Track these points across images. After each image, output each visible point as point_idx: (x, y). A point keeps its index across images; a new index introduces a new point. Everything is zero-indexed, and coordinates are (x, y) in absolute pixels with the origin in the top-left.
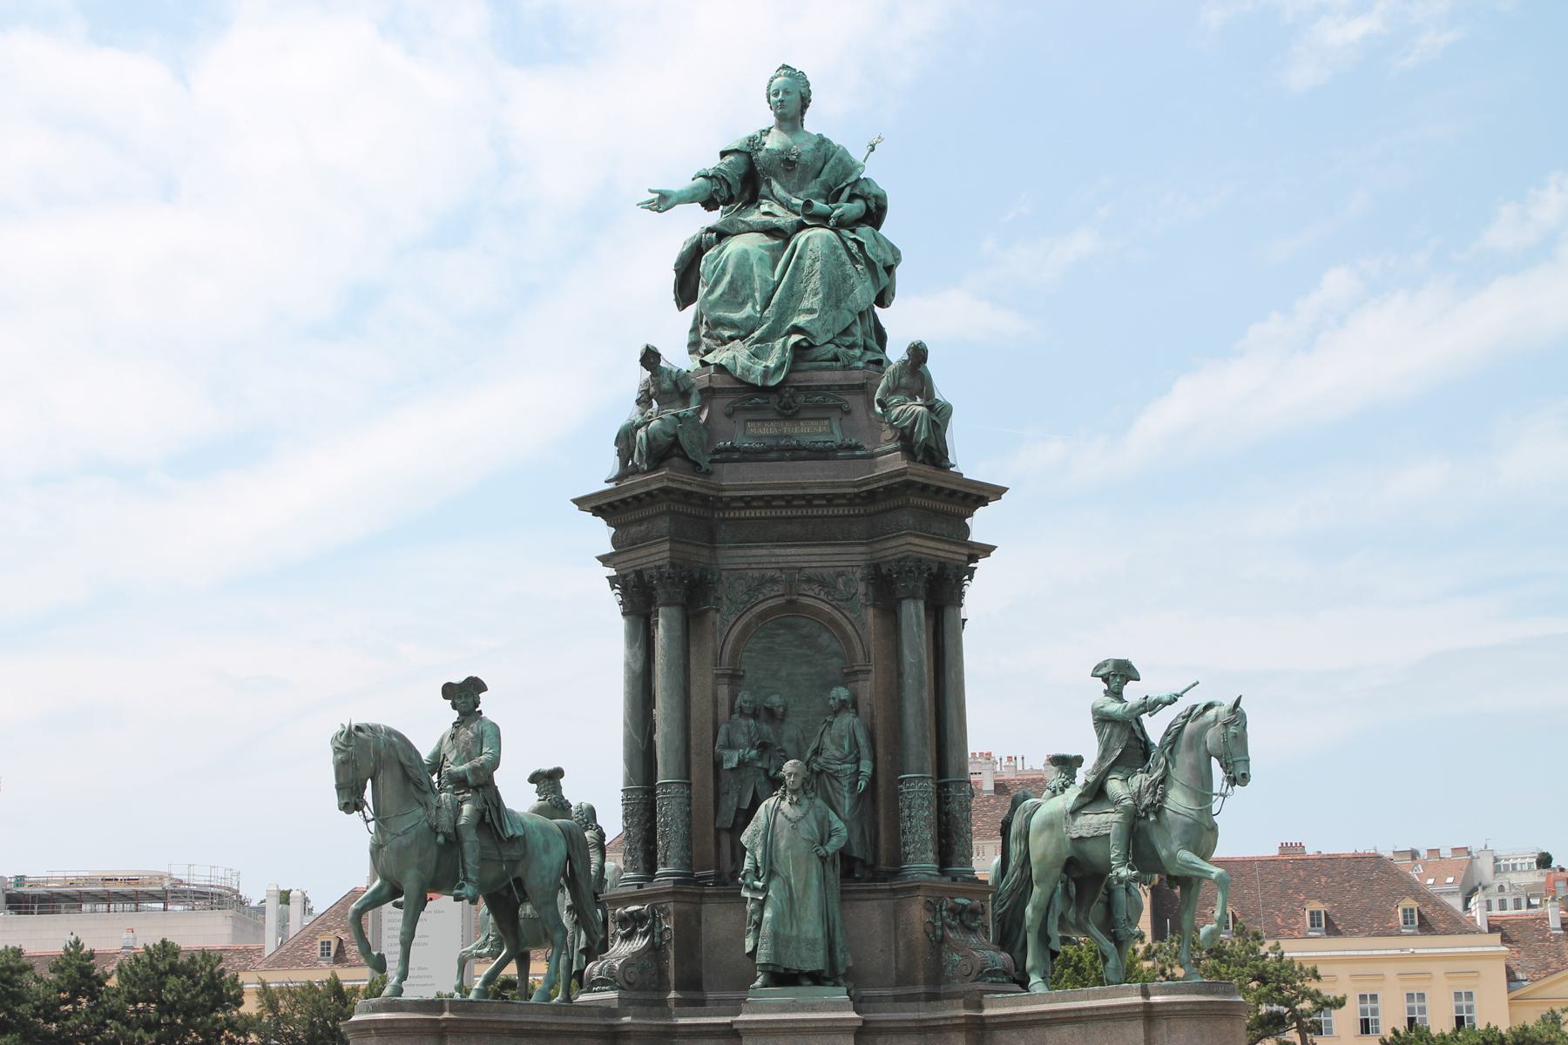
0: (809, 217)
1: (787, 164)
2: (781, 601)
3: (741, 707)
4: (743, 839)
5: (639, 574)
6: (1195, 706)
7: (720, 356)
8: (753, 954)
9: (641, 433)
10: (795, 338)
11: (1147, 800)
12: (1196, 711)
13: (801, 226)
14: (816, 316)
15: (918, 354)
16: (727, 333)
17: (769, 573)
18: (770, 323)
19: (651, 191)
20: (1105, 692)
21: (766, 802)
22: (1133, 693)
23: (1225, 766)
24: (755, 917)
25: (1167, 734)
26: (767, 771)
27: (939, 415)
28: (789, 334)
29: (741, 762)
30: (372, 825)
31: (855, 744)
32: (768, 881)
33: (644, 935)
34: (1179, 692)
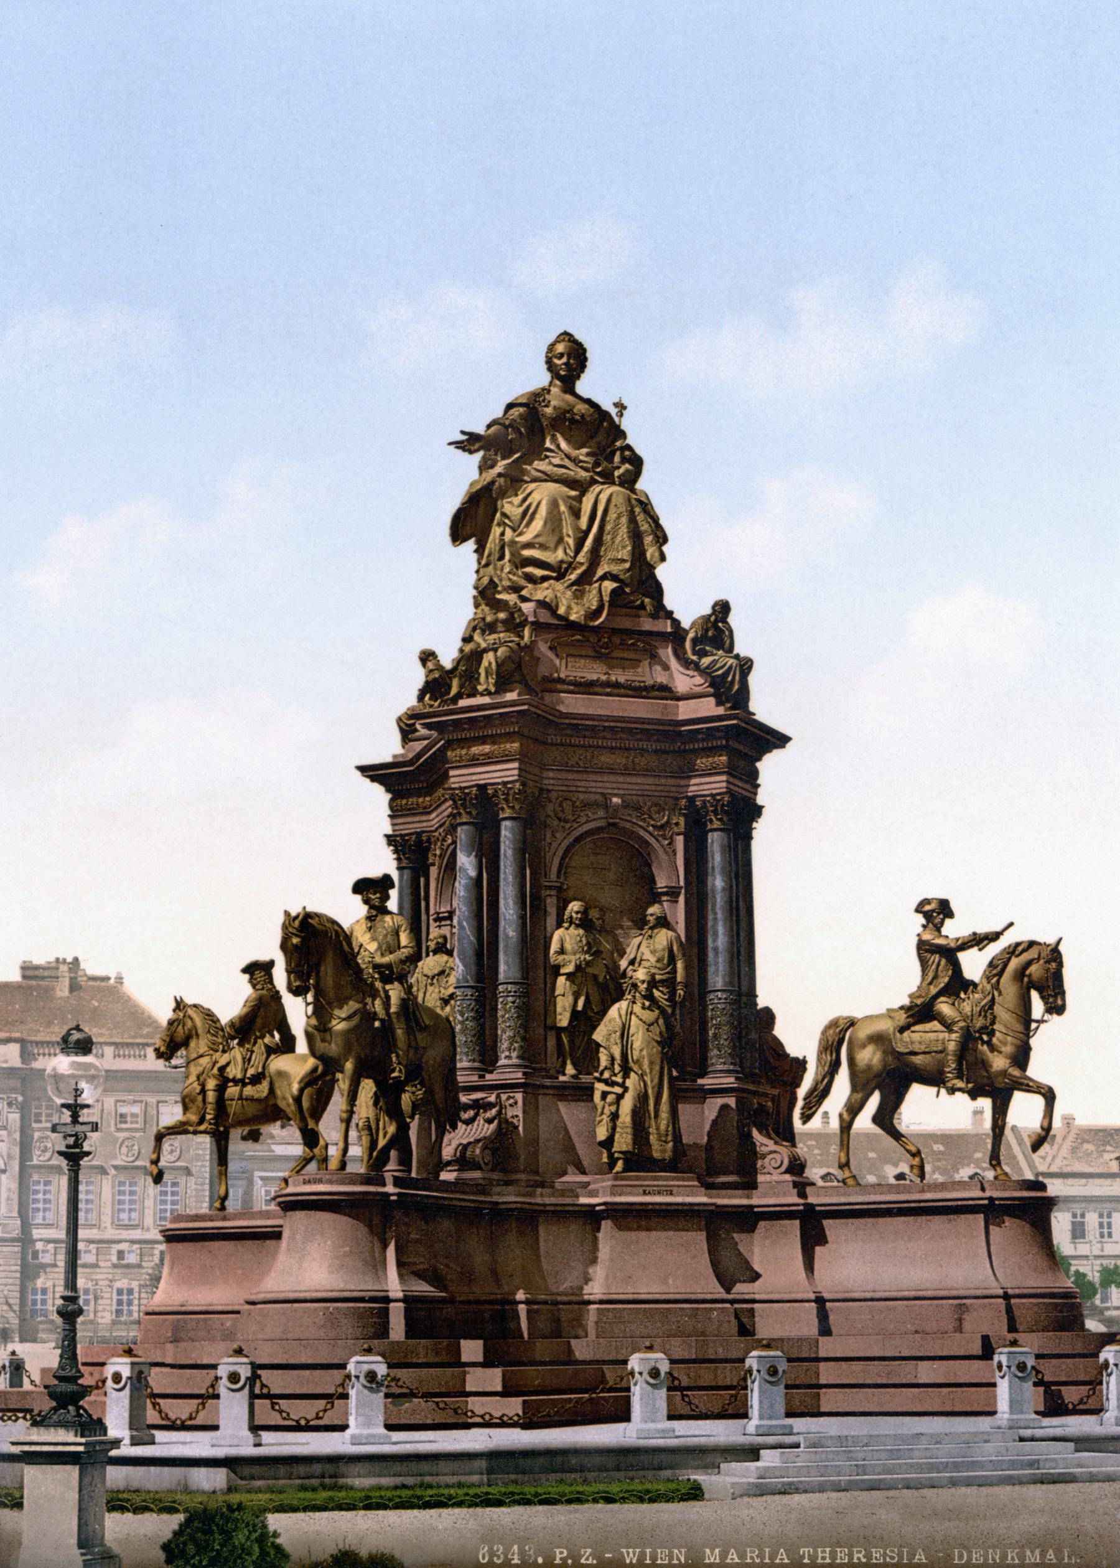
0: (598, 474)
1: (566, 422)
2: (602, 823)
3: (571, 917)
4: (598, 1036)
5: (482, 788)
6: (1018, 944)
7: (543, 593)
8: (608, 1143)
9: (489, 658)
10: (609, 586)
11: (979, 1023)
12: (1020, 948)
13: (593, 482)
14: (627, 565)
15: (723, 609)
16: (539, 572)
17: (593, 797)
18: (583, 568)
19: (463, 432)
20: (924, 927)
21: (617, 1006)
22: (953, 930)
23: (1042, 998)
24: (613, 1108)
25: (991, 965)
26: (595, 977)
27: (746, 666)
28: (603, 578)
29: (578, 968)
30: (310, 1009)
31: (672, 959)
32: (626, 1076)
33: (489, 1121)
34: (998, 929)
